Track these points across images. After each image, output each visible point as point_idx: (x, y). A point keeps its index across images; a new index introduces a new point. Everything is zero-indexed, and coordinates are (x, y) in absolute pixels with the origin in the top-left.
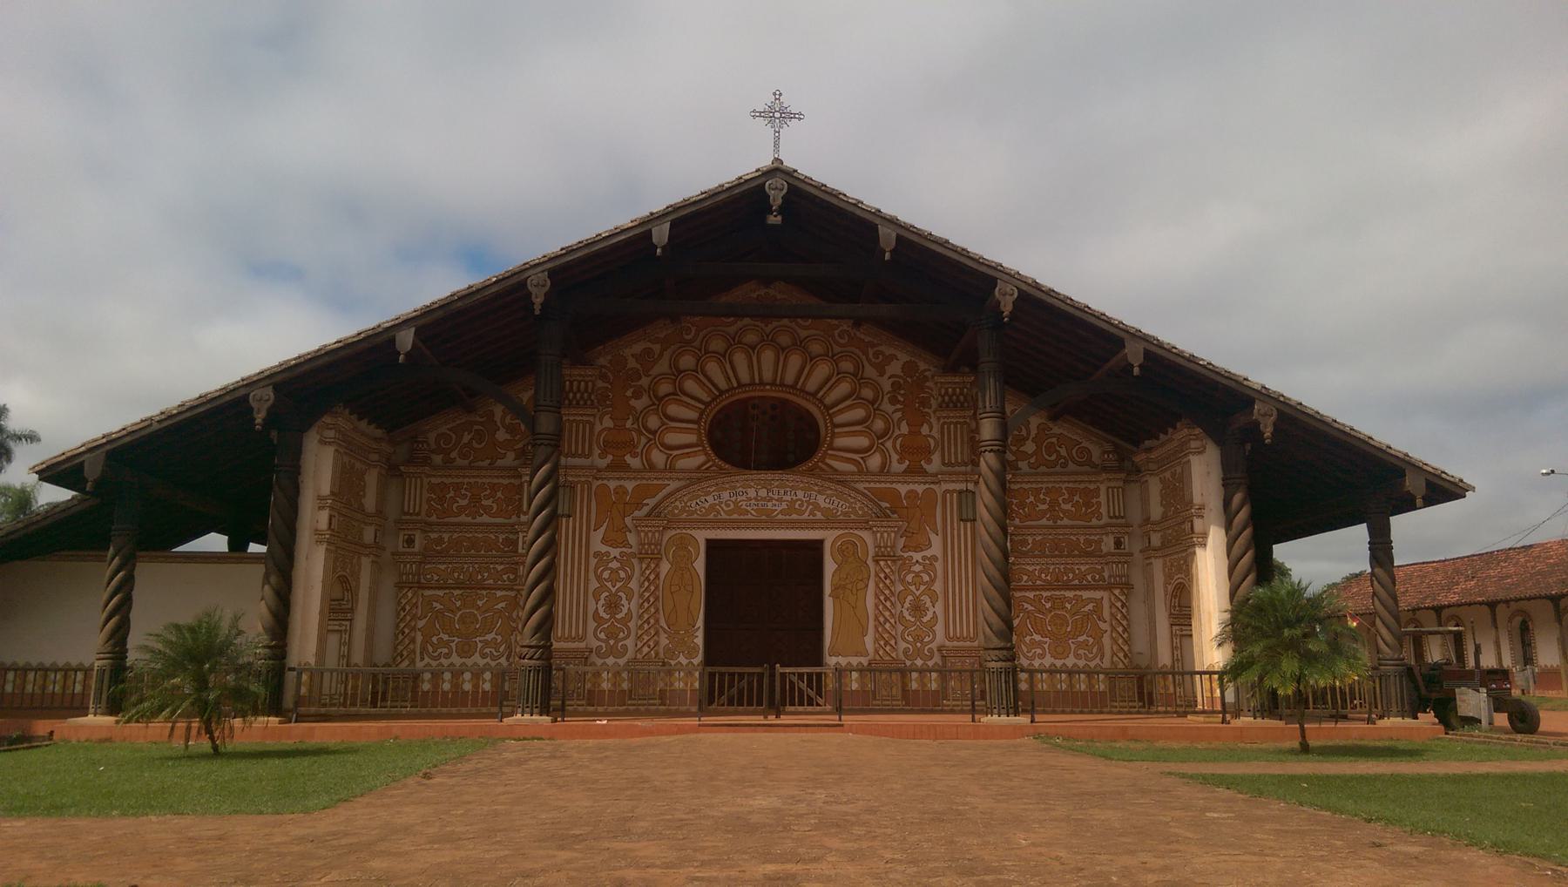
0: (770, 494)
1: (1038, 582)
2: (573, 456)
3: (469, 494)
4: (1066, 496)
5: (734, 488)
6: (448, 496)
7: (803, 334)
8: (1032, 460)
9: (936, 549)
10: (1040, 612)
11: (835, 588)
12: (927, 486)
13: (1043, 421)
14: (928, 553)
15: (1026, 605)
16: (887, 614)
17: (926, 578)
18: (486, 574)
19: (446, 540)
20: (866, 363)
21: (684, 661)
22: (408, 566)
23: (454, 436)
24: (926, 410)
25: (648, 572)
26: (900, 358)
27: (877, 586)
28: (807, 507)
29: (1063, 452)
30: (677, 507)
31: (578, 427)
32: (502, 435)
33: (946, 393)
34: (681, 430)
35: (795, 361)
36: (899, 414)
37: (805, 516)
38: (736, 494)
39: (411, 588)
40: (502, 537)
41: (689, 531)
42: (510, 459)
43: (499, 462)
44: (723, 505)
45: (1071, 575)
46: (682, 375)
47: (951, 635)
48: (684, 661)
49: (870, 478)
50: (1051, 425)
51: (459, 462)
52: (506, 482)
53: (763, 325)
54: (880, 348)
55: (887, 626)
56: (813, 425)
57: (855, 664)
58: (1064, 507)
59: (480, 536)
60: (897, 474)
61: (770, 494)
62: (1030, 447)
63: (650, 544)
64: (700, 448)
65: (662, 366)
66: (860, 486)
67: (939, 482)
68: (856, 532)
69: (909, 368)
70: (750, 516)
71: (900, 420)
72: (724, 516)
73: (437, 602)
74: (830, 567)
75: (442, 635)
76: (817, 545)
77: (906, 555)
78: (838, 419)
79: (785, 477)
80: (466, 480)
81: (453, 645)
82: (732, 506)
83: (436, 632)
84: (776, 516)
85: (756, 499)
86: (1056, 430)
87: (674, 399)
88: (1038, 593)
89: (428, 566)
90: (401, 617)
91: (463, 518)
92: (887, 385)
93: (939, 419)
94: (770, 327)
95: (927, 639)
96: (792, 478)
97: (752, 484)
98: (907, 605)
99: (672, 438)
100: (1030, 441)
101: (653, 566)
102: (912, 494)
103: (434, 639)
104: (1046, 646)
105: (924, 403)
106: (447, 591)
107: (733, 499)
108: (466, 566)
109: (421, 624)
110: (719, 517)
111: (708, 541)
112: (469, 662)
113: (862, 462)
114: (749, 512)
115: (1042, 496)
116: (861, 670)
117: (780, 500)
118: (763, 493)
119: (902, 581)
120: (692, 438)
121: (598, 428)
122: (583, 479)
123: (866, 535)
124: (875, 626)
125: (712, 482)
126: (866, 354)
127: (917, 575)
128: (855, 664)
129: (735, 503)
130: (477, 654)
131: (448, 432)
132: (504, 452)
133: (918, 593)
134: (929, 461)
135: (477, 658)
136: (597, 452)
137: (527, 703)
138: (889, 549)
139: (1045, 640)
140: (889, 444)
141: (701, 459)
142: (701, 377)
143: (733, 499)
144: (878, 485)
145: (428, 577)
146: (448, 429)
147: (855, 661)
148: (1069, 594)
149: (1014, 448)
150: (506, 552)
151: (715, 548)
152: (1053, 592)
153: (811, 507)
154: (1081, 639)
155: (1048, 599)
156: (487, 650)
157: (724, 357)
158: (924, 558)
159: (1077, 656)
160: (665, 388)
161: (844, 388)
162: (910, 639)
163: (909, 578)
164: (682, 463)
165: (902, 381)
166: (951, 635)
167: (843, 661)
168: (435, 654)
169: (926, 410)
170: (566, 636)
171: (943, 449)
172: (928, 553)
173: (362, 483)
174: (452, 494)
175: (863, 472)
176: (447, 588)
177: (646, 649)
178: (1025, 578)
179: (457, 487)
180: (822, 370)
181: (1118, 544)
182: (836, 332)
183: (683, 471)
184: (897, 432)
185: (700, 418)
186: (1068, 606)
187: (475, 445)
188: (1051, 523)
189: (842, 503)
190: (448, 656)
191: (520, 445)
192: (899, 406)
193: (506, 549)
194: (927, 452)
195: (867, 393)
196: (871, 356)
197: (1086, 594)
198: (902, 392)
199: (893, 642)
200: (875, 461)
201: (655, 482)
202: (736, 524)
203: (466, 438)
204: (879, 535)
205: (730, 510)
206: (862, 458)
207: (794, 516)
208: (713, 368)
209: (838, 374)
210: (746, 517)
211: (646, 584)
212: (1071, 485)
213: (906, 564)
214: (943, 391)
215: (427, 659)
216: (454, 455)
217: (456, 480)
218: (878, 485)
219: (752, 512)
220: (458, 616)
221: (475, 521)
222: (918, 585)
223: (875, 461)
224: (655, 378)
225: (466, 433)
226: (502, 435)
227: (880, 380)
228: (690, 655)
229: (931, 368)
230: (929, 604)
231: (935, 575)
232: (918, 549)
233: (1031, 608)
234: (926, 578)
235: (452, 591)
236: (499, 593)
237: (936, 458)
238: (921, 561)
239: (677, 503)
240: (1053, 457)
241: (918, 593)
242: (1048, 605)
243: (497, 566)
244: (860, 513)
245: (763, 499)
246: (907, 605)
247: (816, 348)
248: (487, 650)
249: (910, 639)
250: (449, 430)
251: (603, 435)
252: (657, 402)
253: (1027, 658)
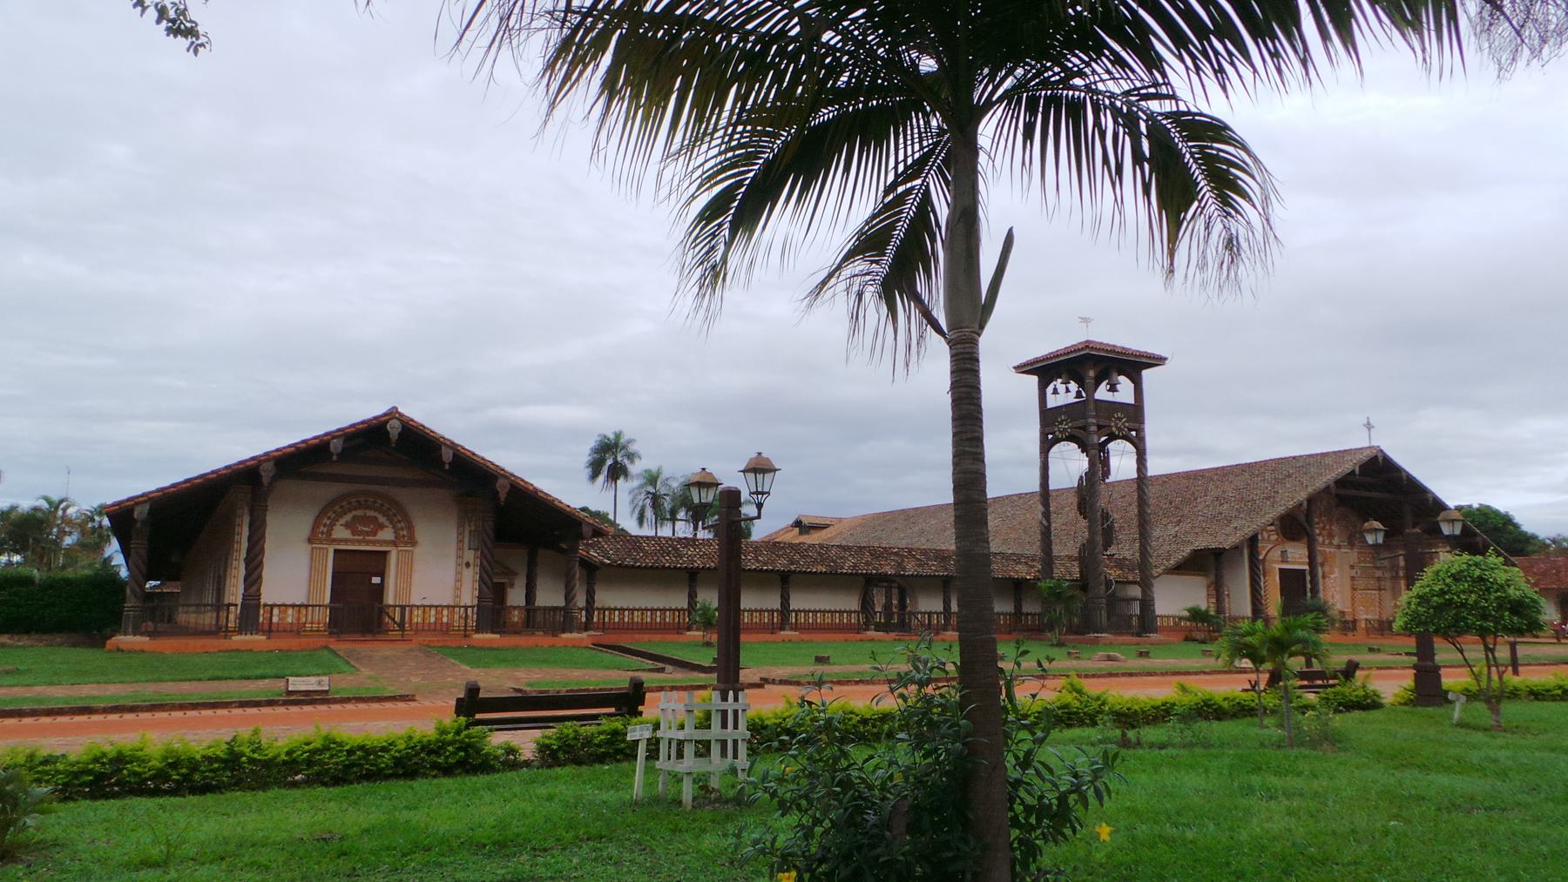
148: (1369, 592)
181: (1397, 573)
197: (1373, 592)
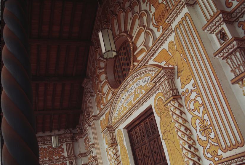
47: (224, 146)
74: (158, 119)
77: (184, 90)
84: (133, 103)
98: (198, 128)
133: (200, 115)
162: (209, 156)
163: (192, 107)
166: (224, 146)
173: (61, 149)
189: (148, 77)
207: (138, 99)
222: (198, 108)
232: (187, 82)
238: (193, 89)
241: (200, 115)
246: (198, 128)
249: (209, 156)
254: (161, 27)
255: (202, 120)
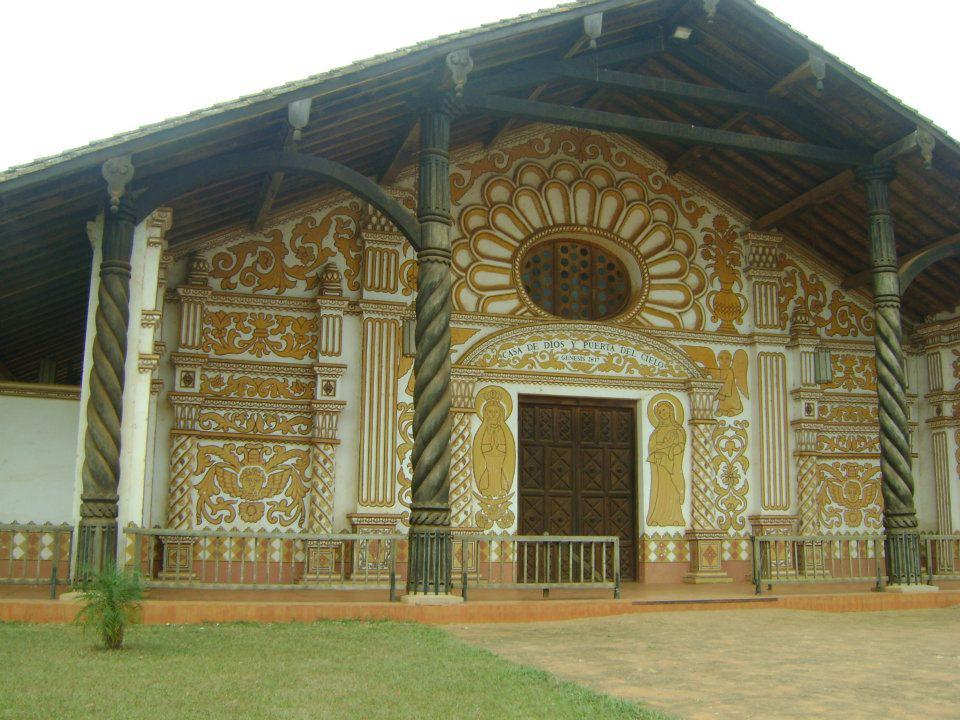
0: (587, 347)
1: (837, 451)
2: (378, 289)
3: (254, 328)
4: (859, 365)
5: (550, 338)
6: (229, 328)
7: (619, 175)
8: (829, 327)
9: (747, 414)
10: (838, 480)
11: (653, 453)
12: (739, 347)
13: (837, 288)
14: (740, 418)
15: (826, 473)
16: (707, 481)
17: (738, 444)
18: (273, 424)
19: (225, 381)
20: (680, 214)
21: (496, 529)
22: (187, 409)
23: (234, 258)
24: (736, 268)
25: (462, 428)
26: (712, 210)
27: (695, 450)
28: (624, 364)
29: (853, 320)
30: (488, 356)
31: (381, 256)
32: (291, 260)
33: (757, 252)
34: (493, 269)
35: (610, 204)
36: (711, 271)
37: (623, 374)
38: (552, 345)
39: (190, 436)
40: (291, 380)
41: (500, 384)
42: (300, 290)
43: (288, 292)
44: (538, 357)
45: (863, 444)
46: (496, 207)
48: (496, 529)
49: (685, 335)
50: (843, 294)
51: (241, 289)
52: (296, 315)
53: (577, 161)
54: (691, 199)
55: (708, 493)
56: (624, 274)
57: (672, 534)
58: (857, 375)
59: (266, 377)
60: (711, 333)
61: (587, 347)
62: (826, 314)
63: (463, 397)
64: (514, 291)
65: (472, 196)
66: (676, 344)
67: (753, 344)
68: (672, 393)
69: (719, 222)
70: (566, 371)
71: (713, 277)
72: (539, 369)
73: (215, 454)
74: (646, 429)
75: (222, 494)
76: (628, 409)
77: (719, 419)
78: (654, 270)
79: (603, 328)
80: (249, 311)
81: (236, 507)
82: (547, 359)
83: (216, 491)
84: (594, 370)
85: (572, 351)
86: (848, 298)
87: (486, 233)
88: (836, 461)
89: (205, 411)
90: (178, 471)
91: (246, 356)
92: (699, 237)
93: (749, 278)
94: (585, 164)
95: (739, 508)
96: (609, 329)
97: (568, 334)
98: (720, 472)
99: (483, 278)
100: (825, 309)
101: (467, 421)
102: (725, 355)
103: (214, 499)
104: (842, 514)
105: (735, 260)
106: (228, 442)
107: (549, 350)
108: (249, 413)
109: (197, 480)
110: (534, 369)
111: (520, 396)
112: (255, 527)
113: (678, 317)
114: (564, 365)
115: (839, 364)
116: (676, 537)
117: (597, 354)
118: (579, 345)
119: (716, 447)
120: (504, 279)
121: (402, 260)
122: (390, 317)
123: (682, 397)
124: (693, 493)
125: (527, 329)
126: (679, 203)
127: (730, 440)
128: (672, 534)
129: (551, 355)
130: (264, 519)
131: (228, 252)
132: (294, 280)
133: (730, 459)
134: (740, 322)
135: (264, 523)
136: (401, 287)
137: (431, 577)
138: (708, 412)
139: (842, 508)
140: (703, 301)
141: (514, 303)
142: (516, 211)
143: (549, 350)
144: (692, 344)
145: (206, 424)
146: (228, 249)
147: (672, 530)
148: (861, 462)
149: (813, 314)
150: (298, 398)
151: (526, 401)
152: (849, 461)
153: (628, 363)
154: (870, 507)
155: (845, 467)
156: (276, 514)
157: (567, 188)
158: (737, 423)
159: (867, 524)
160: (476, 221)
161: (658, 238)
162: (724, 507)
163: (723, 444)
164: (495, 307)
165: (713, 236)
167: (661, 531)
168: (215, 517)
169: (736, 268)
170: (381, 498)
171: (755, 305)
172: (740, 418)
174: (233, 326)
175: (678, 328)
176: (228, 438)
177: (462, 517)
178: (826, 445)
179: (240, 318)
180: (636, 217)
182: (650, 177)
183: (498, 316)
184: (711, 289)
185: (514, 256)
186: (860, 474)
187: (259, 269)
188: (846, 391)
189: (659, 360)
190: (229, 519)
191: (312, 274)
192: (711, 261)
193: (297, 395)
194: (736, 312)
195: (681, 245)
196: (684, 206)
198: (714, 247)
199: (712, 511)
200: (689, 319)
201: (464, 326)
202: (553, 379)
203: (249, 261)
204: (698, 397)
205: (545, 363)
206: (679, 313)
207: (612, 373)
208: (526, 202)
209: (654, 222)
210: (561, 371)
211: (461, 441)
212: (862, 354)
213: (719, 429)
214: (754, 249)
215: (205, 523)
216: (235, 279)
217: (237, 310)
218: (692, 344)
219: (569, 366)
220: (241, 472)
221: (259, 359)
223: (689, 319)
224: (466, 208)
225: (249, 255)
226: (291, 260)
227: (692, 231)
228: (505, 524)
229: (742, 226)
230: (741, 472)
231: (746, 438)
232: (730, 412)
233: (829, 476)
234: (738, 444)
235: (234, 442)
236: (289, 447)
237: (747, 318)
239: (489, 351)
240: (846, 326)
241: (730, 459)
242: (844, 473)
243: (286, 415)
244: (677, 372)
245: (580, 352)
246: (720, 472)
247: (631, 193)
248: (276, 514)
249: (724, 507)
250: (228, 249)
251: (407, 269)
252: (468, 236)
253: (826, 525)
254: (720, 322)
255: (730, 466)
